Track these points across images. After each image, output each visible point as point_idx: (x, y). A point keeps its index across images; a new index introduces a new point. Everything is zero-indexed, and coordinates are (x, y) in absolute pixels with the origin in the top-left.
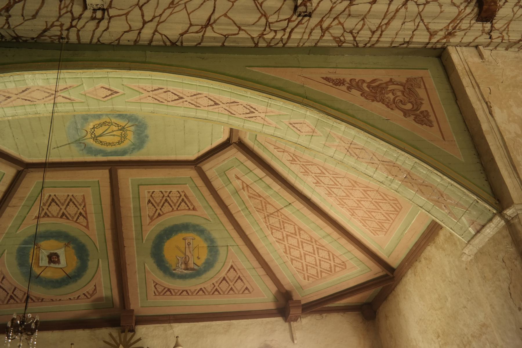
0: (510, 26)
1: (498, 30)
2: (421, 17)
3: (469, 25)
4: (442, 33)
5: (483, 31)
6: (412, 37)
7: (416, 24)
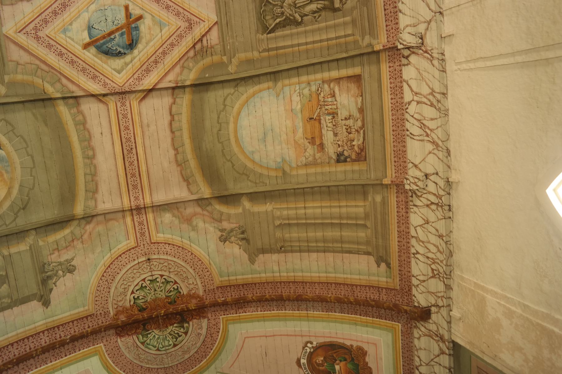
0: (432, 291)
1: (436, 301)
2: (430, 362)
3: (434, 324)
4: (441, 344)
5: (437, 313)
6: (446, 367)
7: (435, 364)
